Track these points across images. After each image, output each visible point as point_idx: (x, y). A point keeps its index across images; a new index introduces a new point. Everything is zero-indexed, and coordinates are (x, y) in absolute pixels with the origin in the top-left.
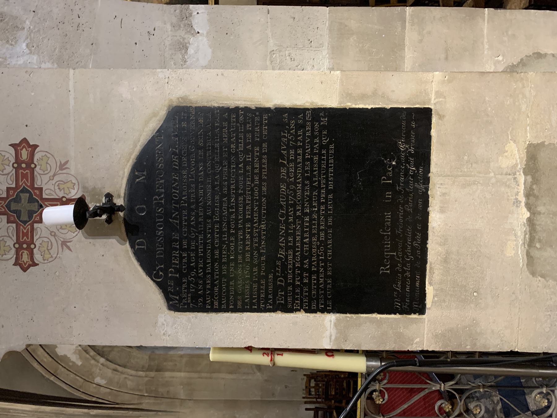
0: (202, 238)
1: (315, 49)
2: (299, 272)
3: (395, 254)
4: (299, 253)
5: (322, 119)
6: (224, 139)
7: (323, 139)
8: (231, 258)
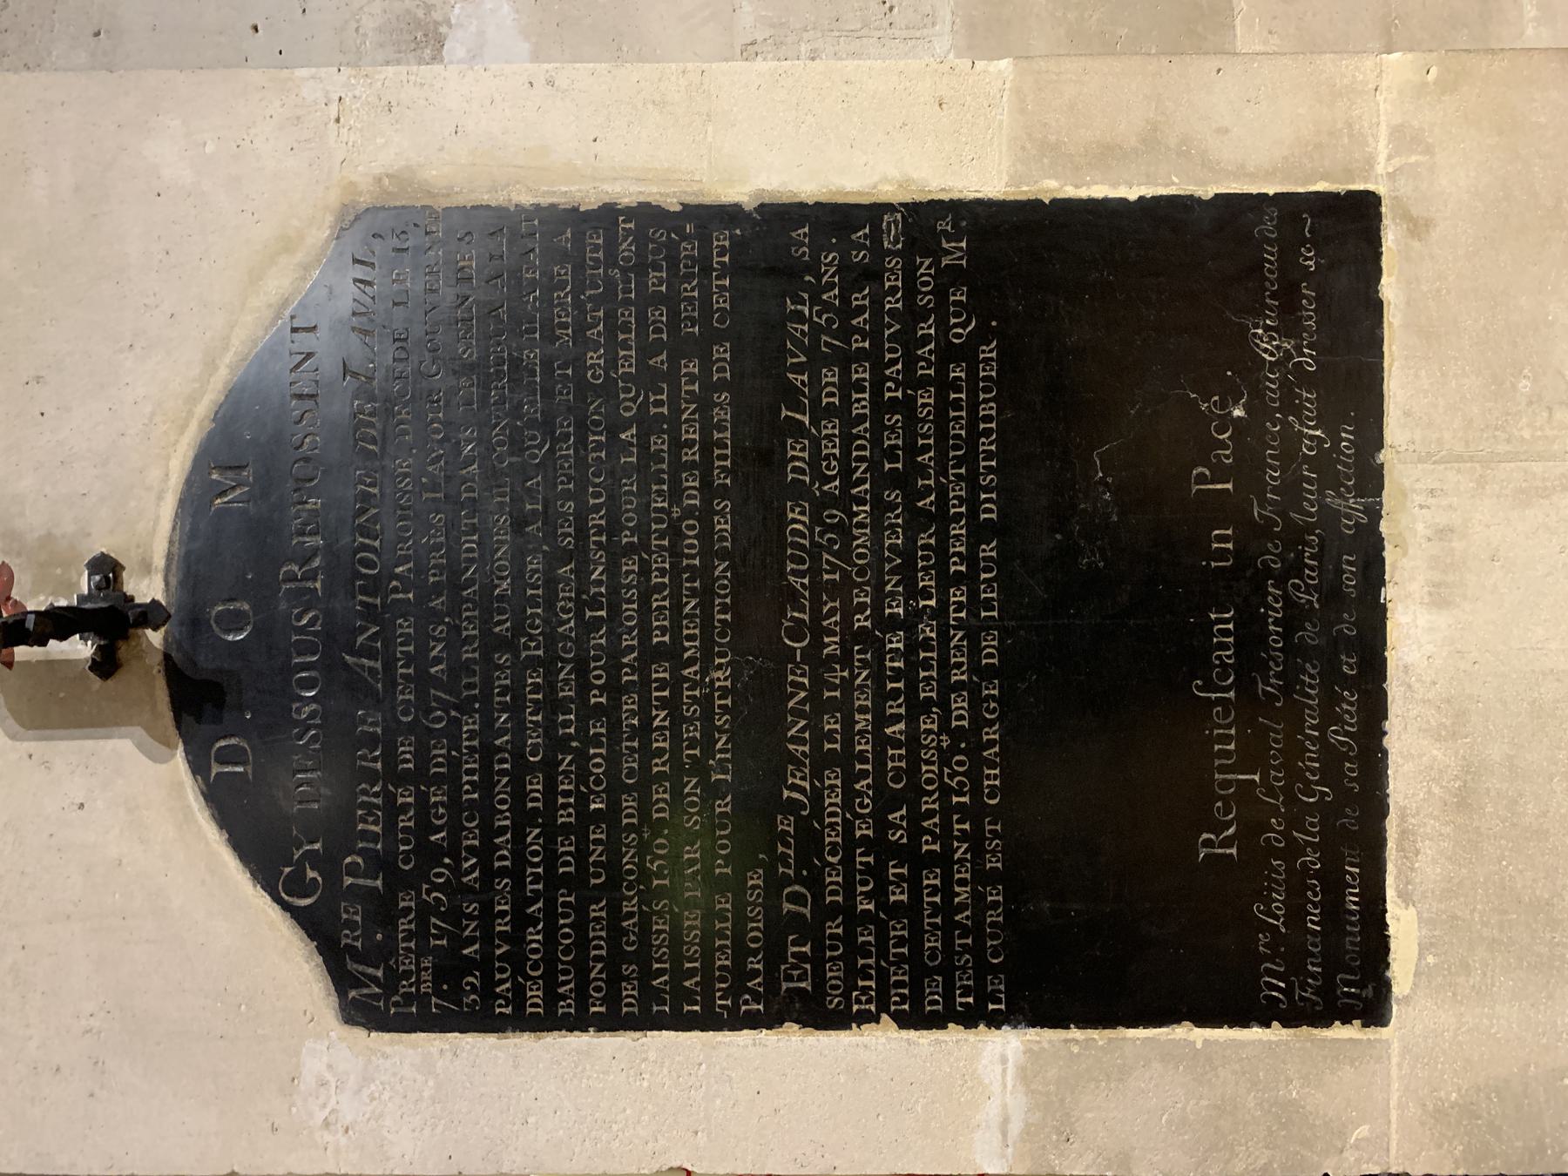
0: (477, 727)
1: (905, 34)
2: (871, 859)
3: (1257, 778)
4: (870, 781)
5: (945, 245)
6: (558, 332)
7: (953, 321)
8: (593, 806)
